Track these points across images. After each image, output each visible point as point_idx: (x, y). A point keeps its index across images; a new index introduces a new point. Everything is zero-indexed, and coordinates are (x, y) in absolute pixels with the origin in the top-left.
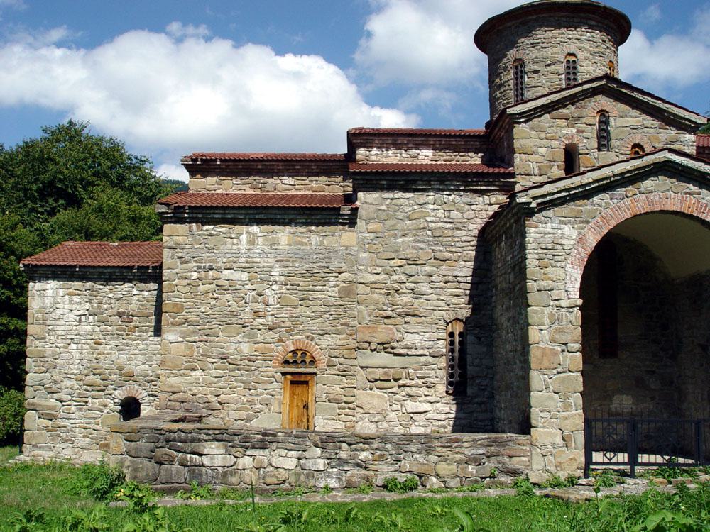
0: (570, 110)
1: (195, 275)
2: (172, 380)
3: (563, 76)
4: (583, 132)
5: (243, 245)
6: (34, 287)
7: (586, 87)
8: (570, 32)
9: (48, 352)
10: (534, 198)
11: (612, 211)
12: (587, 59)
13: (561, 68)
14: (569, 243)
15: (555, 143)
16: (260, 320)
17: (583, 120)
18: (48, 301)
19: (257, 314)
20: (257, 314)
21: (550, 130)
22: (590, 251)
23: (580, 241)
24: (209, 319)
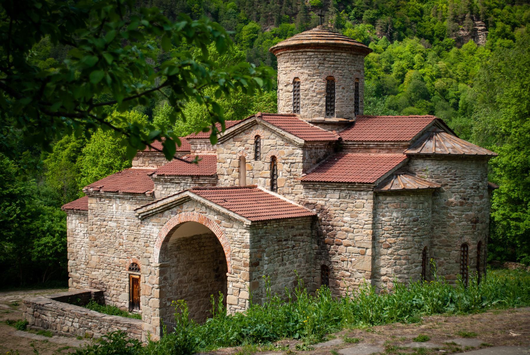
1: (99, 223)
2: (93, 273)
3: (292, 93)
4: (248, 149)
5: (114, 210)
6: (69, 219)
7: (247, 122)
8: (296, 63)
9: (74, 250)
10: (139, 214)
11: (173, 220)
12: (306, 80)
13: (291, 88)
14: (155, 235)
15: (234, 156)
16: (121, 247)
17: (248, 142)
18: (73, 225)
21: (232, 148)
22: (163, 240)
23: (160, 235)
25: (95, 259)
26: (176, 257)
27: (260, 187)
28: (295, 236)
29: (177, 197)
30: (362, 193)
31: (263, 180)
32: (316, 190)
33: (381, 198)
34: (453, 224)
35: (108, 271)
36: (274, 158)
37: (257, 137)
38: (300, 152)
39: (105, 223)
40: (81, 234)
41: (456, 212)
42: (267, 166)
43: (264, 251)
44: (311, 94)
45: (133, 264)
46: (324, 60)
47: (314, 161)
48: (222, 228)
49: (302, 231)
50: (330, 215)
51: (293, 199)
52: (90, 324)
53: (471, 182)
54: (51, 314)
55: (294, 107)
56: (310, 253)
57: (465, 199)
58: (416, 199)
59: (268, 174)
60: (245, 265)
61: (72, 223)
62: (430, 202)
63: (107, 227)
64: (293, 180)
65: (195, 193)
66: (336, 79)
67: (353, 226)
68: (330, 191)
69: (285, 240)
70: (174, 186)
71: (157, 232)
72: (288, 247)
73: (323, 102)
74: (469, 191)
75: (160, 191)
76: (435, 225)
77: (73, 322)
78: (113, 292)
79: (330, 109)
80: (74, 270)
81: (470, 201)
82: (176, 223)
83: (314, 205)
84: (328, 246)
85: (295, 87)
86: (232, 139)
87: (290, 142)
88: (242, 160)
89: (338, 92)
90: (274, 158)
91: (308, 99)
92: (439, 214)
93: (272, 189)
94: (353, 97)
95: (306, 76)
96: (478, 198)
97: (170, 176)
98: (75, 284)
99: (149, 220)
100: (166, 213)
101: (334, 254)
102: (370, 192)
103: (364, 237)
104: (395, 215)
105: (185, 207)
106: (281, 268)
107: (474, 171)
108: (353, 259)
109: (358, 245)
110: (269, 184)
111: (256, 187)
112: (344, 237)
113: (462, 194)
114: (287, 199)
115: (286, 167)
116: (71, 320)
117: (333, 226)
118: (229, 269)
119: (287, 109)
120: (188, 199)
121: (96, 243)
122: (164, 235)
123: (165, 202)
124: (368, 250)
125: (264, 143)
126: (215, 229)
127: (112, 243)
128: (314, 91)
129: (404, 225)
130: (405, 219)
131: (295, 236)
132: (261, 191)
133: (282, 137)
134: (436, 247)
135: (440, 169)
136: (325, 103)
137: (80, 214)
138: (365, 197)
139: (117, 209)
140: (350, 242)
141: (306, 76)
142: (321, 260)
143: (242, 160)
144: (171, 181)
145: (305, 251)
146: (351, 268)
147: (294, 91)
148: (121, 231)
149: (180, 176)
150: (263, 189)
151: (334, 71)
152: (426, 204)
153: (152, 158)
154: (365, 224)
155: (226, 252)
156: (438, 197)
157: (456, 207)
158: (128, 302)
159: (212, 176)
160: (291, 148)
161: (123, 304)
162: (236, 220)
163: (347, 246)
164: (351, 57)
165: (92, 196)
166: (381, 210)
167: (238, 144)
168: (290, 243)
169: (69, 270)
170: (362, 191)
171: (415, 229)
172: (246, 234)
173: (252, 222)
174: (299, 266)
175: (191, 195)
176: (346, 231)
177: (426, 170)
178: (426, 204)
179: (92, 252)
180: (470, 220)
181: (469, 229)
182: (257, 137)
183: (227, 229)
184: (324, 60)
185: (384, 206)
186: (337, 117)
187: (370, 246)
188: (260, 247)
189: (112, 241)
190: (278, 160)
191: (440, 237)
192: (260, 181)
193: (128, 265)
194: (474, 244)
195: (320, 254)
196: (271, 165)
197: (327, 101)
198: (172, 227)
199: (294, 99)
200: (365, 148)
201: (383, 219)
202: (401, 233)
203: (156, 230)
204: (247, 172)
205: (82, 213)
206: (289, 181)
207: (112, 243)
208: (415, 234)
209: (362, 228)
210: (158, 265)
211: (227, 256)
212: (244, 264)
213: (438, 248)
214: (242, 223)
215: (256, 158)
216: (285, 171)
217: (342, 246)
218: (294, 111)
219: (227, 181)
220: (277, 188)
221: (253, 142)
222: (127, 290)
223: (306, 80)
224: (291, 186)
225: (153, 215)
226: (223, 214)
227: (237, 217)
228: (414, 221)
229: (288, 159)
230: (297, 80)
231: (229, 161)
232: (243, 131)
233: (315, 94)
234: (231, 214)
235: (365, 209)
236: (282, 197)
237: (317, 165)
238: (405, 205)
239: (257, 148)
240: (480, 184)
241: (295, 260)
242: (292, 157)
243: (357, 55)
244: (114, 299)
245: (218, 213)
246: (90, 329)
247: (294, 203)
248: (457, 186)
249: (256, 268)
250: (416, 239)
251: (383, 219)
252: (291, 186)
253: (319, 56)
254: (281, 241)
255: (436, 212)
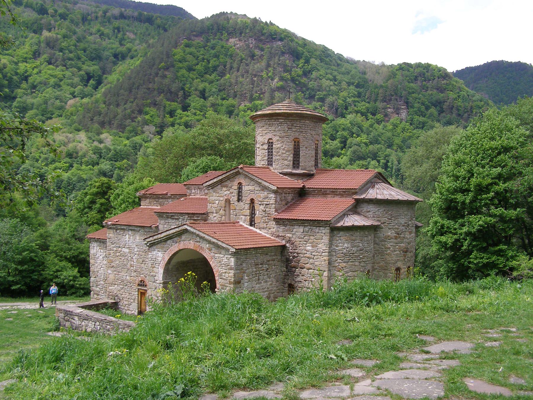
0: (228, 183)
2: (110, 288)
4: (232, 193)
5: (127, 239)
7: (232, 172)
11: (174, 248)
13: (266, 147)
14: (160, 259)
16: (132, 268)
17: (233, 187)
18: (95, 251)
19: (131, 266)
20: (131, 266)
23: (163, 258)
24: (118, 266)
25: (112, 277)
26: (176, 276)
27: (241, 223)
28: (269, 261)
29: (177, 230)
30: (321, 228)
31: (243, 217)
32: (285, 225)
33: (335, 232)
34: (389, 253)
35: (122, 286)
36: (252, 201)
37: (240, 184)
38: (272, 195)
39: (120, 249)
40: (101, 257)
41: (391, 244)
42: (247, 206)
43: (244, 272)
44: (281, 151)
45: (141, 281)
46: (292, 125)
47: (284, 203)
48: (212, 254)
49: (274, 257)
50: (296, 246)
51: (267, 234)
52: (108, 326)
53: (403, 221)
54: (78, 318)
55: (268, 161)
56: (280, 275)
57: (398, 234)
58: (362, 233)
59: (248, 212)
60: (230, 283)
61: (94, 249)
62: (373, 235)
63: (121, 252)
64: (267, 218)
65: (191, 227)
66: (301, 141)
67: (313, 254)
68: (296, 227)
69: (261, 264)
70: (174, 221)
71: (161, 257)
72: (263, 270)
73: (291, 158)
74: (401, 228)
75: (163, 225)
76: (376, 253)
77: (95, 325)
78: (126, 303)
79: (296, 163)
80: (95, 285)
81: (402, 236)
82: (177, 249)
83: (284, 237)
84: (294, 269)
85: (269, 146)
86: (220, 186)
87: (264, 188)
88: (228, 201)
89: (303, 150)
90: (252, 201)
91: (279, 155)
92: (379, 245)
93: (251, 225)
94: (314, 155)
95: (278, 138)
96: (408, 233)
97: (171, 213)
98: (96, 296)
99: (155, 247)
100: (169, 242)
101: (298, 275)
102: (327, 228)
103: (322, 262)
104: (346, 245)
105: (183, 237)
106: (258, 285)
107: (405, 213)
108: (313, 279)
109: (317, 268)
110: (249, 220)
111: (239, 222)
112: (306, 262)
113: (396, 230)
114: (263, 232)
115: (262, 207)
116: (93, 323)
117: (298, 254)
118: (218, 286)
119: (263, 163)
120: (186, 231)
121: (113, 264)
122: (167, 258)
123: (168, 233)
124: (325, 273)
125: (245, 188)
126: (207, 255)
127: (125, 265)
128: (284, 149)
129: (353, 253)
130: (353, 249)
131: (269, 261)
132: (241, 225)
133: (259, 184)
134: (376, 270)
135: (380, 211)
136: (292, 159)
137: (100, 242)
138: (324, 231)
139: (129, 238)
140: (311, 266)
141: (278, 138)
142: (288, 279)
143: (228, 201)
144: (172, 217)
145: (276, 273)
146: (311, 286)
147: (268, 149)
148: (132, 255)
149: (178, 213)
150: (243, 224)
151: (299, 135)
152: (370, 237)
153: (157, 200)
154: (323, 252)
155: (215, 273)
156: (378, 232)
157: (392, 240)
158: (137, 311)
159: (204, 214)
160: (266, 193)
161: (133, 312)
162: (223, 248)
163: (308, 269)
164: (312, 124)
165: (111, 228)
166: (335, 242)
167: (224, 189)
168: (264, 266)
169: (91, 285)
170: (320, 227)
171: (361, 257)
172: (231, 259)
173: (236, 249)
174: (271, 284)
175: (189, 228)
176: (308, 258)
177: (369, 211)
178: (370, 237)
179: (109, 272)
180: (402, 250)
181: (401, 257)
182: (240, 184)
183: (216, 255)
184: (292, 125)
185: (338, 238)
186: (301, 170)
187: (327, 270)
188: (242, 269)
189: (125, 263)
190: (256, 202)
191: (379, 263)
192: (241, 218)
193: (137, 282)
194: (404, 268)
195: (288, 275)
196: (250, 206)
197: (294, 157)
198: (173, 252)
199: (268, 155)
200: (323, 194)
201: (337, 248)
202: (350, 259)
203: (160, 254)
204: (232, 211)
205: (102, 242)
206: (264, 218)
207: (125, 265)
208: (361, 261)
209: (321, 255)
210: (162, 282)
211: (216, 275)
212: (229, 282)
213: (378, 271)
214: (228, 250)
215: (239, 200)
216: (261, 211)
217: (305, 269)
218: (268, 164)
219: (216, 218)
220: (255, 224)
221: (236, 188)
222: (136, 301)
223: (278, 140)
224: (266, 222)
225: (158, 244)
226: (214, 243)
227: (224, 245)
228: (361, 250)
229: (264, 201)
230: (271, 141)
231: (217, 202)
232: (229, 179)
233: (284, 152)
234: (220, 243)
235: (323, 241)
236: (258, 231)
237: (286, 206)
238: (354, 238)
239: (239, 192)
240: (410, 222)
241: (268, 279)
242: (267, 200)
243: (317, 122)
244: (126, 308)
245: (210, 242)
246: (109, 330)
247: (268, 236)
248: (393, 224)
249: (238, 286)
250: (362, 264)
251: (337, 248)
252: (266, 222)
253: (288, 123)
254: (258, 265)
255: (377, 244)
